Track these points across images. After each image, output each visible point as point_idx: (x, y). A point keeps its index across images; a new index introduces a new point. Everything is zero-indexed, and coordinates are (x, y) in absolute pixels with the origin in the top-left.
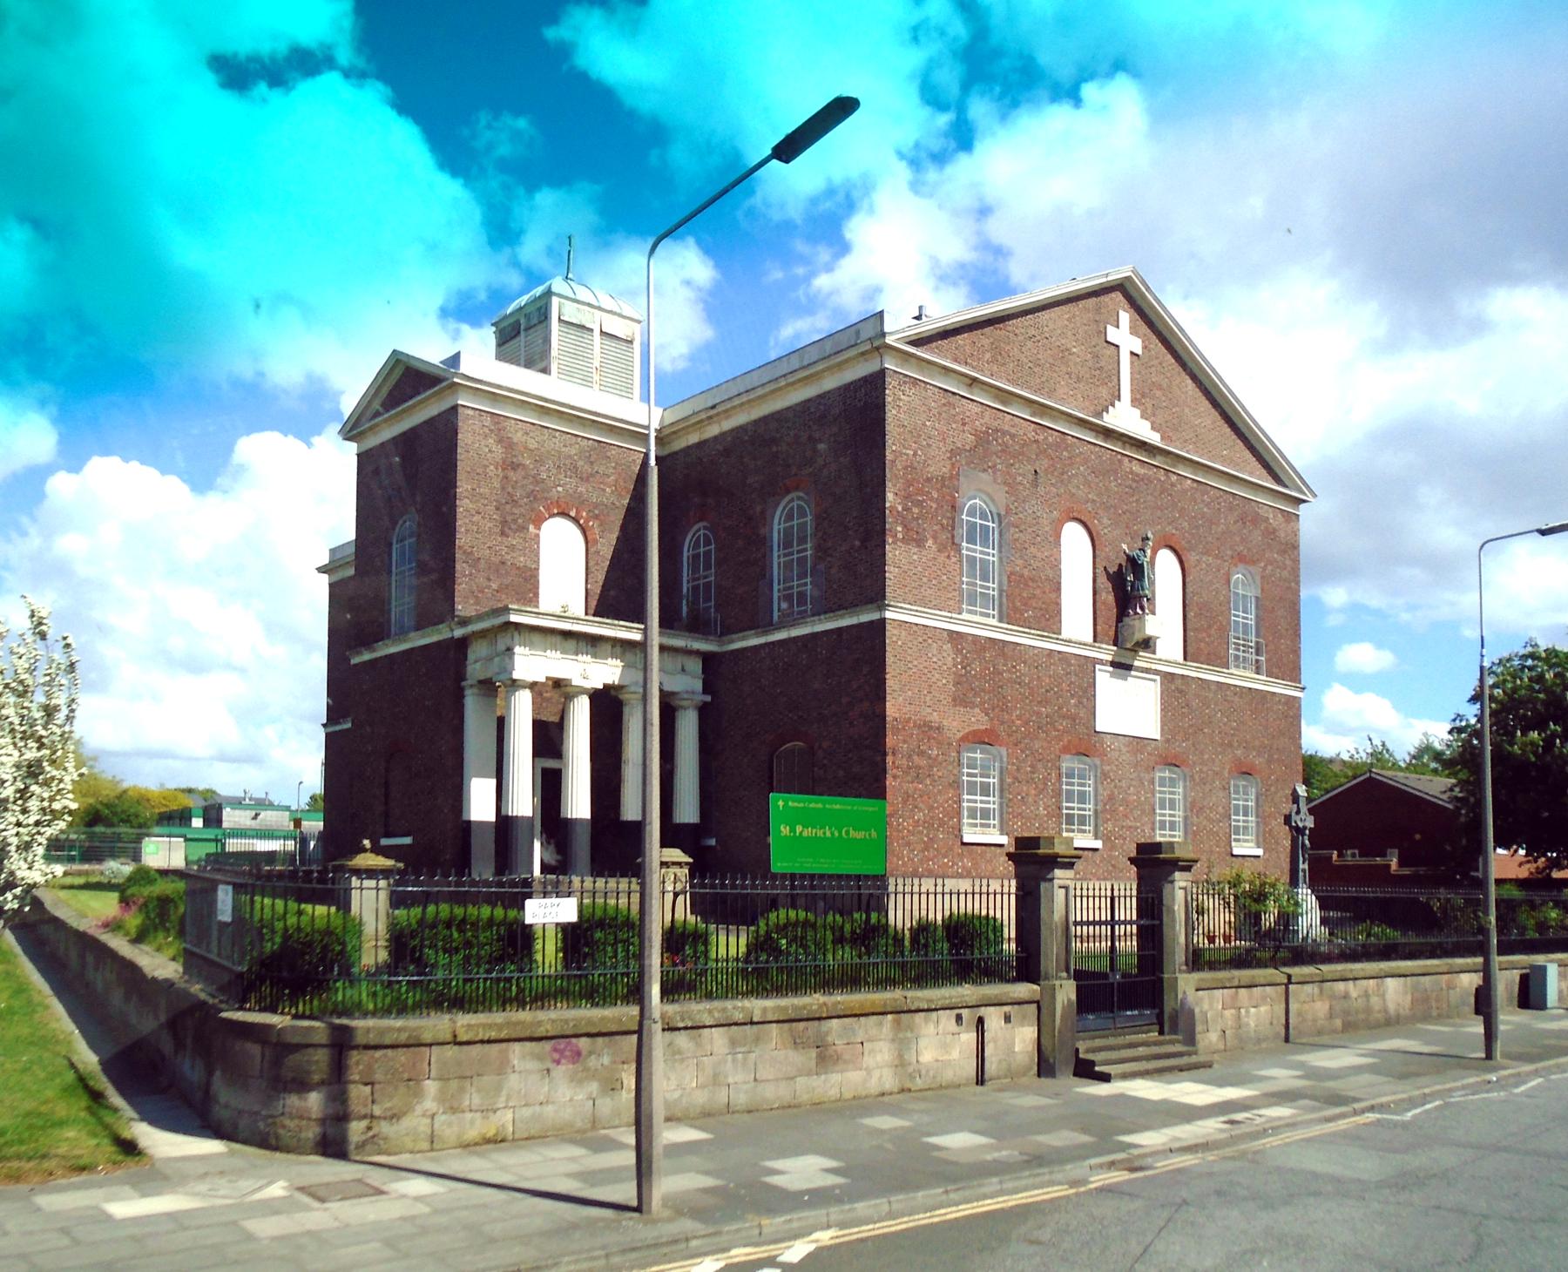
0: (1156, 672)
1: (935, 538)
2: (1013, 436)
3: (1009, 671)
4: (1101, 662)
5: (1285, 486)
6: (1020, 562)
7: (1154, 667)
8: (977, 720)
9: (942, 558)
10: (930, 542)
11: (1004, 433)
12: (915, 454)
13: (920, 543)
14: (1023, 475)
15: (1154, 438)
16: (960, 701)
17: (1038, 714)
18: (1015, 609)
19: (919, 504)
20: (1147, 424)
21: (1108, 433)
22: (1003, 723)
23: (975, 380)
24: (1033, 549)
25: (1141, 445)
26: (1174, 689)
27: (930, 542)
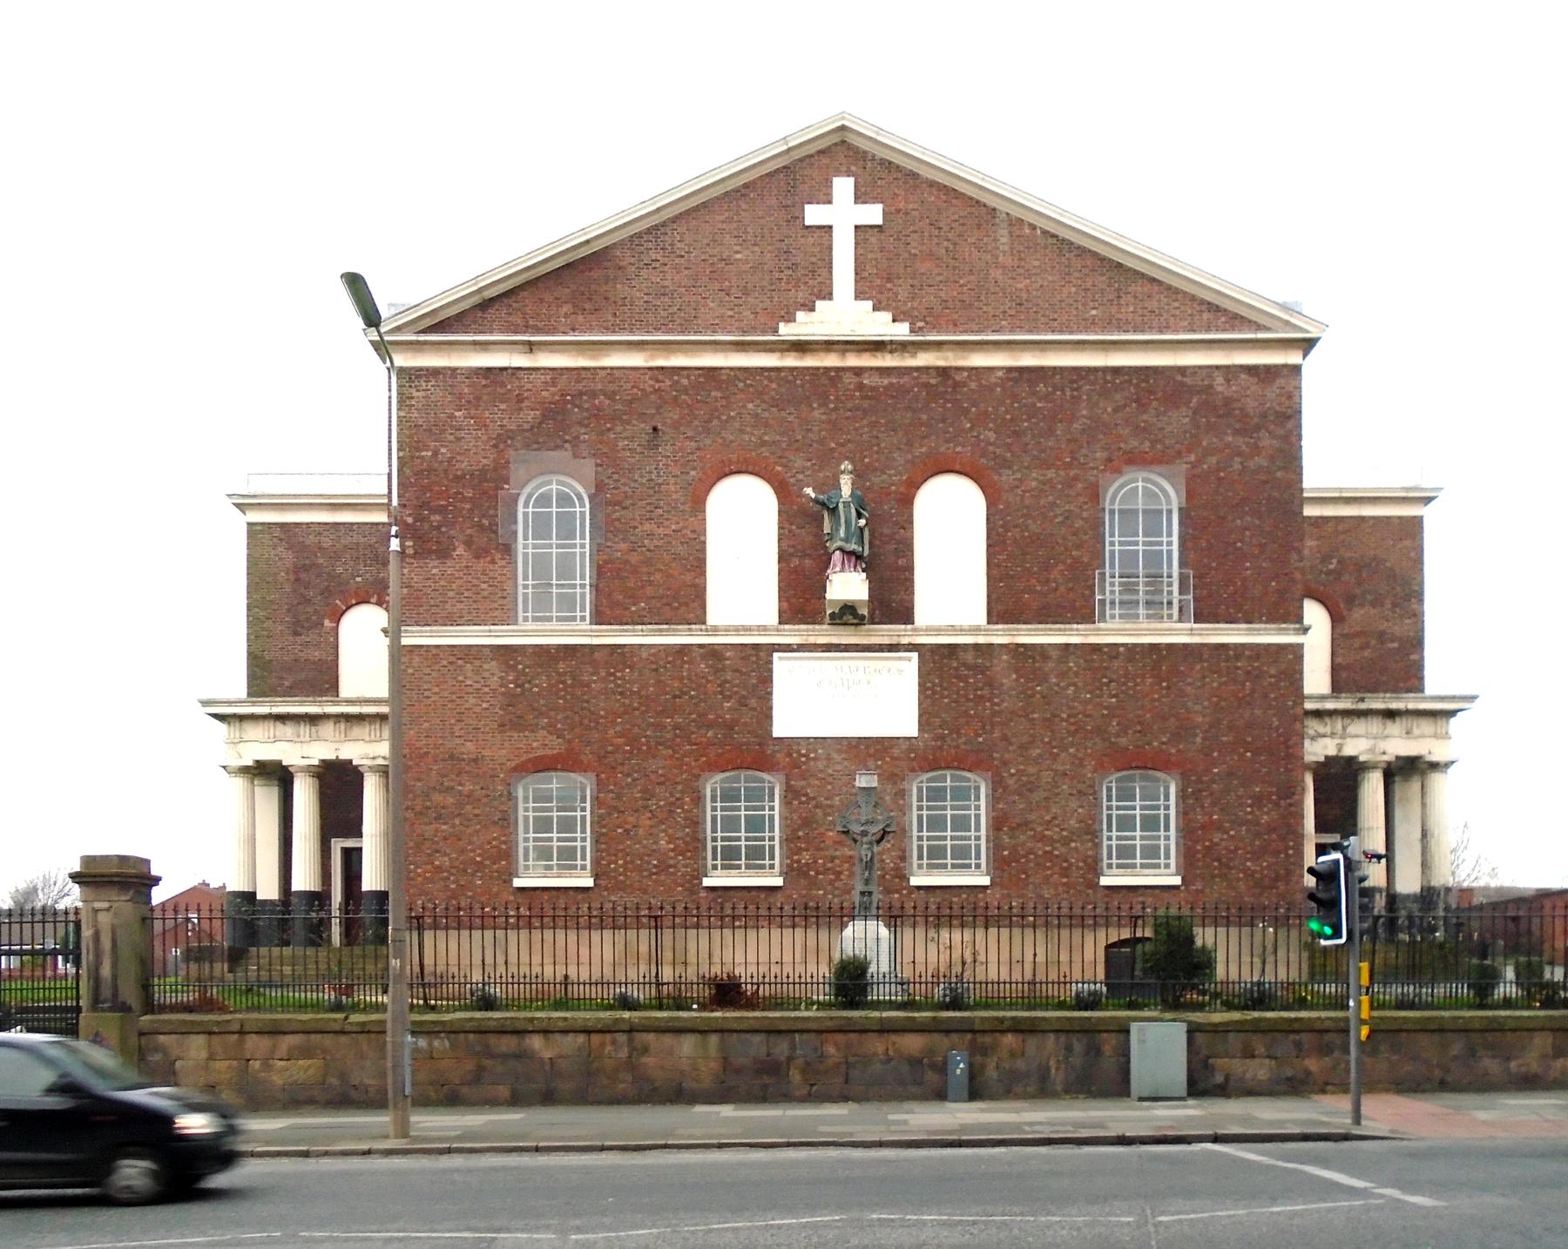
0: (912, 647)
1: (468, 543)
2: (611, 396)
3: (603, 680)
4: (787, 648)
5: (1268, 329)
6: (623, 546)
7: (905, 641)
8: (543, 742)
9: (481, 565)
10: (460, 550)
11: (593, 394)
12: (436, 453)
13: (444, 554)
14: (631, 439)
15: (901, 331)
16: (514, 723)
17: (659, 727)
18: (614, 605)
19: (441, 510)
20: (888, 316)
21: (801, 347)
22: (589, 743)
23: (530, 343)
24: (647, 527)
25: (877, 346)
26: (944, 668)
27: (460, 550)
